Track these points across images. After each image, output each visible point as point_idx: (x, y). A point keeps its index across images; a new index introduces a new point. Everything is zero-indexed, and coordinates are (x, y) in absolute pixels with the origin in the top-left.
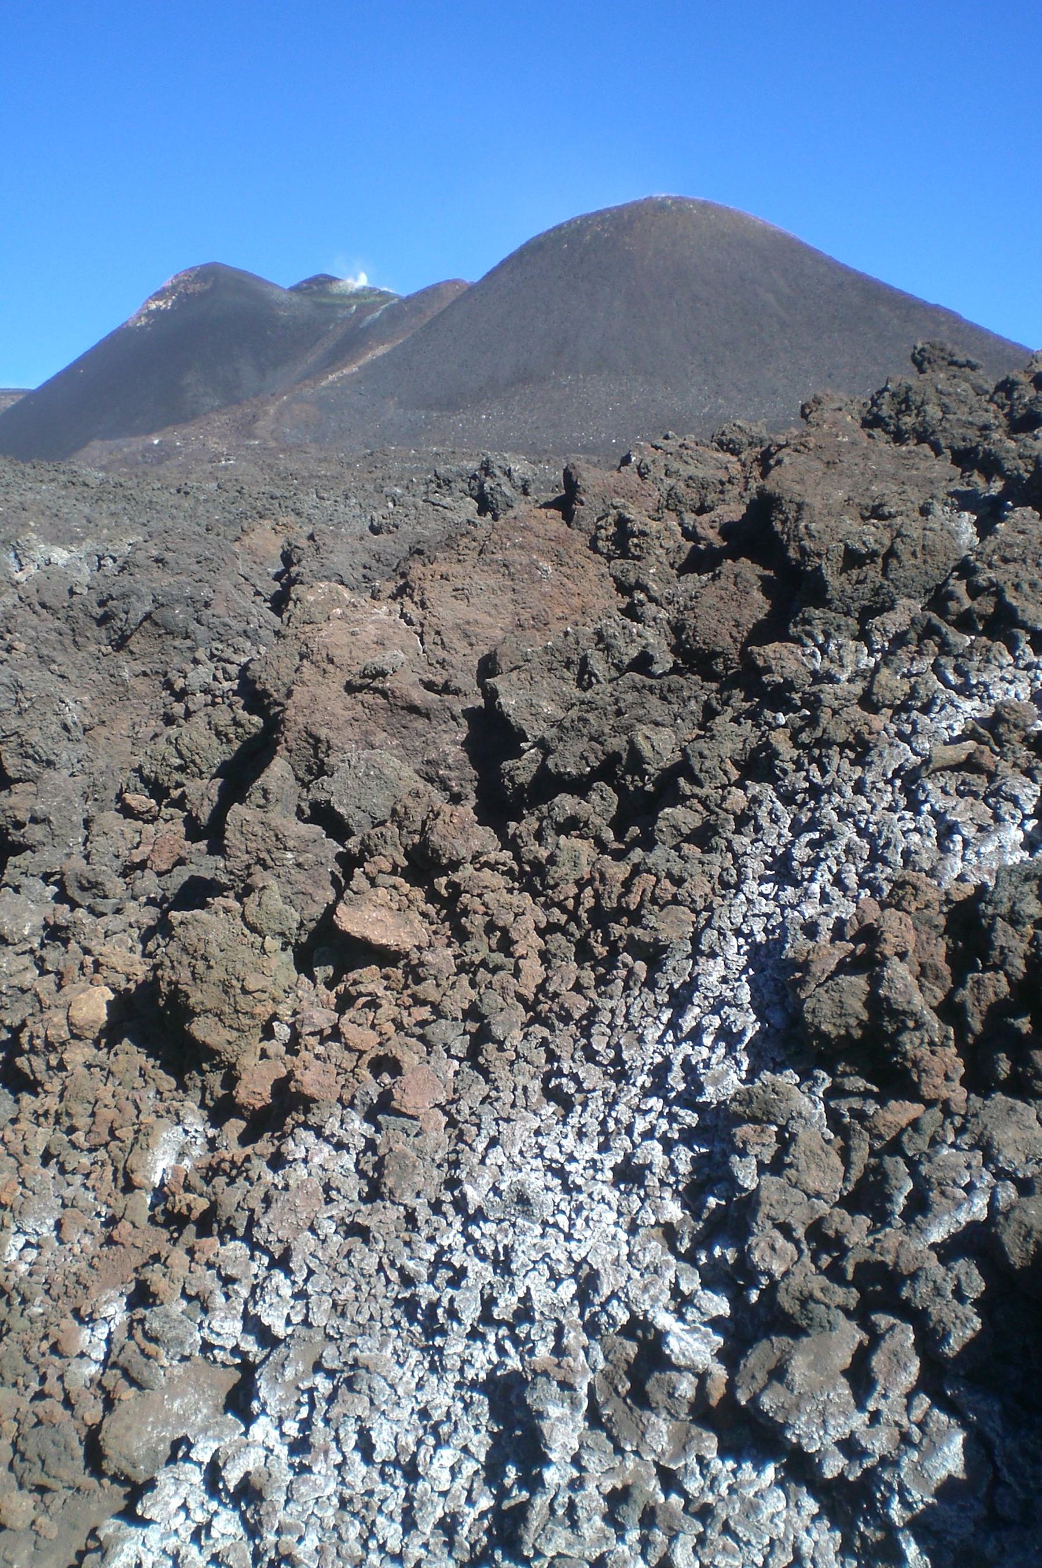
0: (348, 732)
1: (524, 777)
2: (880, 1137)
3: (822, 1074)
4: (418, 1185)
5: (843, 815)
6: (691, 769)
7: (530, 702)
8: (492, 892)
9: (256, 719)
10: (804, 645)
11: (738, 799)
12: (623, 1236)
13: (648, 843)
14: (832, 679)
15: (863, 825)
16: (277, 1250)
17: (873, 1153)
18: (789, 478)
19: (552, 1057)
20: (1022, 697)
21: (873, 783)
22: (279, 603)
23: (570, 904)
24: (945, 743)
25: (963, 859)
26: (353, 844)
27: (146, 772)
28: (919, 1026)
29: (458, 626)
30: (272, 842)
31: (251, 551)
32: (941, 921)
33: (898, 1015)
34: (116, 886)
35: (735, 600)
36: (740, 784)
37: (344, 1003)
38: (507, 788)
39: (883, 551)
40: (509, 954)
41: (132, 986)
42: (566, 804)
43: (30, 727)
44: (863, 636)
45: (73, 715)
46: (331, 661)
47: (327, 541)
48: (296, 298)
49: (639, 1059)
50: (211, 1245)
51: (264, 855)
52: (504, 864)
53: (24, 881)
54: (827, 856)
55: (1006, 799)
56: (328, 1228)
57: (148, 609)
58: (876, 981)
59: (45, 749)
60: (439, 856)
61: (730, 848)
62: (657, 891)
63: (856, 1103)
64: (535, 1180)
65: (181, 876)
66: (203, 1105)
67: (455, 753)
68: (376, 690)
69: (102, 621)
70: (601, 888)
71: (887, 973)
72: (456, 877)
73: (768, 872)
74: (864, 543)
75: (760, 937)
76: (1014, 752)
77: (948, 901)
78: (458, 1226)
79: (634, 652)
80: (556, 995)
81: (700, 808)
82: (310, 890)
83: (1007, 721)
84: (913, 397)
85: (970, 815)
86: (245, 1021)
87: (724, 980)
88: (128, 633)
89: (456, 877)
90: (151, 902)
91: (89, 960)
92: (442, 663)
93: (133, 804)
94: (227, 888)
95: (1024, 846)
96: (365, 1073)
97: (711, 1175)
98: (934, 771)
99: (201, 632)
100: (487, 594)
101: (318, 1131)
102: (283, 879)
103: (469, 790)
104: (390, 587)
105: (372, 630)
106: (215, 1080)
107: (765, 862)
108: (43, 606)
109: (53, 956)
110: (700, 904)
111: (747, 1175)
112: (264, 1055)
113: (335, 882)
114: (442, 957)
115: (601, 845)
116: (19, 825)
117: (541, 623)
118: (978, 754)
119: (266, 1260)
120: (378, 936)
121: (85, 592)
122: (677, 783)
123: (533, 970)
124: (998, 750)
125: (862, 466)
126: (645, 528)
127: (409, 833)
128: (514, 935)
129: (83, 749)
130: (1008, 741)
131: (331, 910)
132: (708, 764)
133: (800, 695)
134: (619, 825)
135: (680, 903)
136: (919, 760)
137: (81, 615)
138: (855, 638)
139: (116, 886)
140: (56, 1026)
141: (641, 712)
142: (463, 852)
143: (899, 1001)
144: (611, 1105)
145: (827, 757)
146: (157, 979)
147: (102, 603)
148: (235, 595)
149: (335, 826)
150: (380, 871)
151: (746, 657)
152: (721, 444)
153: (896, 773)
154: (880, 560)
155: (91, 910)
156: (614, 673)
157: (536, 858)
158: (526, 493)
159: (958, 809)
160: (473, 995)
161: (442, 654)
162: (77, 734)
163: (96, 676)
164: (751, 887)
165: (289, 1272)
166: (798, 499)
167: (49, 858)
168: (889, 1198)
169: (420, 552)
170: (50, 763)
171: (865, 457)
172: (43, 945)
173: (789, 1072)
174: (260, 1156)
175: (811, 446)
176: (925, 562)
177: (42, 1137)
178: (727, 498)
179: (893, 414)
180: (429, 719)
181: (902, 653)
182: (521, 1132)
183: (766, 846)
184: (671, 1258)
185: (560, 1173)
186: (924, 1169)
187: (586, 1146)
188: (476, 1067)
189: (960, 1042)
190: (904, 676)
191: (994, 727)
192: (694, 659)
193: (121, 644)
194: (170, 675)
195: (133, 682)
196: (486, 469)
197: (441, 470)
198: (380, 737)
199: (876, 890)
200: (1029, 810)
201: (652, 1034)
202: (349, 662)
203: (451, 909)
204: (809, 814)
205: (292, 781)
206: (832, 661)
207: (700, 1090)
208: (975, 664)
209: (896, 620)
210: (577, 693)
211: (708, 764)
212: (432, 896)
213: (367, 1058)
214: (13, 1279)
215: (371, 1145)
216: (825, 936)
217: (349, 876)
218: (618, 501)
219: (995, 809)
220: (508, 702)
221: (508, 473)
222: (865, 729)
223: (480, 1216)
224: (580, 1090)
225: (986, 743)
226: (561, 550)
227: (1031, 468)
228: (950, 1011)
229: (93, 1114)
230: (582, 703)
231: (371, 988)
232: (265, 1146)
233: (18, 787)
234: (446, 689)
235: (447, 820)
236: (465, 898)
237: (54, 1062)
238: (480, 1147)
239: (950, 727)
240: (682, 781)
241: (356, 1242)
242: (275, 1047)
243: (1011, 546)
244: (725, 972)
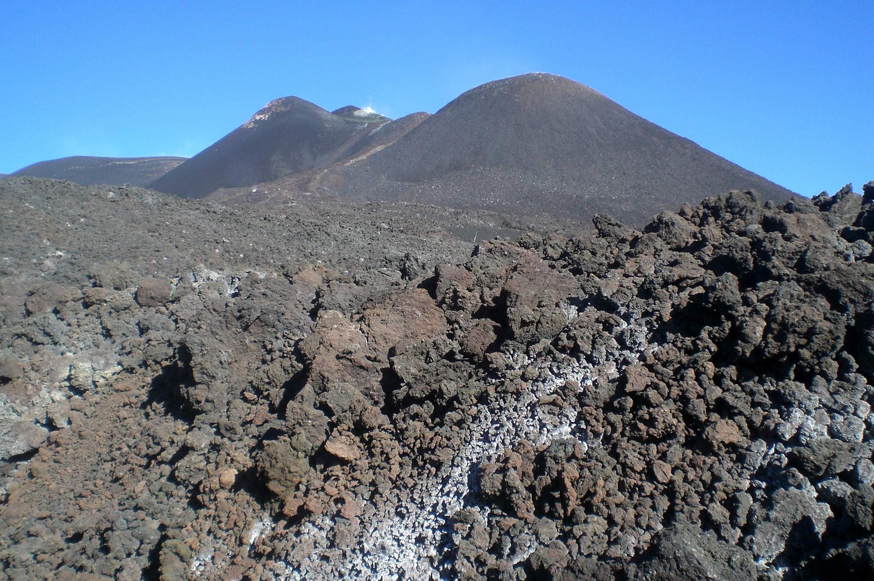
0: (336, 375)
1: (401, 397)
2: (503, 529)
3: (487, 508)
4: (348, 543)
5: (508, 419)
8: (385, 440)
9: (300, 365)
11: (474, 409)
12: (415, 561)
13: (441, 424)
16: (296, 564)
17: (500, 534)
18: (516, 284)
19: (399, 500)
22: (314, 314)
23: (412, 445)
26: (334, 418)
28: (518, 492)
31: (302, 279)
32: (534, 458)
33: (511, 488)
34: (240, 430)
35: (481, 334)
36: (476, 405)
37: (327, 478)
40: (388, 463)
41: (245, 469)
42: (415, 408)
43: (206, 361)
44: (527, 353)
45: (224, 357)
49: (429, 502)
50: (272, 563)
51: (300, 421)
53: (203, 426)
56: (315, 557)
58: (504, 477)
59: (212, 371)
61: (469, 428)
63: (498, 519)
64: (389, 542)
65: (267, 427)
66: (271, 515)
67: (377, 385)
68: (348, 359)
69: (239, 318)
71: (508, 473)
72: (371, 433)
75: (475, 461)
77: (537, 451)
78: (360, 557)
80: (403, 478)
86: (289, 483)
87: (461, 475)
89: (371, 433)
90: (254, 437)
91: (229, 458)
92: (375, 349)
96: (332, 503)
97: (447, 540)
101: (313, 523)
103: (382, 400)
104: (357, 317)
106: (276, 506)
108: (214, 310)
109: (213, 456)
111: (457, 539)
112: (295, 496)
113: (327, 433)
114: (364, 463)
115: (426, 424)
116: (199, 402)
117: (415, 336)
119: (291, 569)
123: (396, 468)
128: (390, 456)
129: (227, 372)
131: (324, 443)
134: (433, 417)
139: (240, 430)
140: (215, 483)
142: (375, 424)
143: (511, 483)
144: (417, 518)
146: (256, 466)
147: (239, 311)
148: (295, 310)
149: (329, 412)
152: (520, 243)
153: (529, 405)
155: (230, 439)
156: (439, 358)
158: (424, 268)
160: (374, 477)
161: (375, 345)
162: (226, 365)
163: (234, 342)
164: (474, 443)
165: (299, 571)
167: (213, 417)
168: (502, 549)
169: (372, 300)
170: (213, 377)
171: (545, 277)
172: (209, 452)
173: (477, 507)
174: (291, 532)
177: (208, 525)
182: (386, 525)
184: (431, 568)
185: (398, 540)
186: (515, 540)
187: (407, 531)
188: (372, 503)
189: (534, 499)
192: (469, 356)
193: (246, 328)
195: (250, 345)
196: (407, 257)
198: (348, 377)
199: (514, 446)
200: (573, 420)
201: (434, 493)
203: (369, 445)
205: (313, 393)
207: (446, 511)
209: (538, 347)
210: (425, 364)
212: (362, 440)
213: (333, 498)
214: (194, 577)
215: (332, 529)
216: (493, 460)
217: (332, 431)
218: (454, 283)
220: (398, 367)
221: (416, 260)
223: (368, 553)
224: (408, 512)
228: (531, 489)
229: (228, 517)
231: (337, 473)
232: (294, 529)
233: (199, 386)
234: (375, 360)
236: (374, 441)
237: (212, 498)
238: (371, 531)
241: (325, 562)
242: (300, 494)
244: (460, 473)
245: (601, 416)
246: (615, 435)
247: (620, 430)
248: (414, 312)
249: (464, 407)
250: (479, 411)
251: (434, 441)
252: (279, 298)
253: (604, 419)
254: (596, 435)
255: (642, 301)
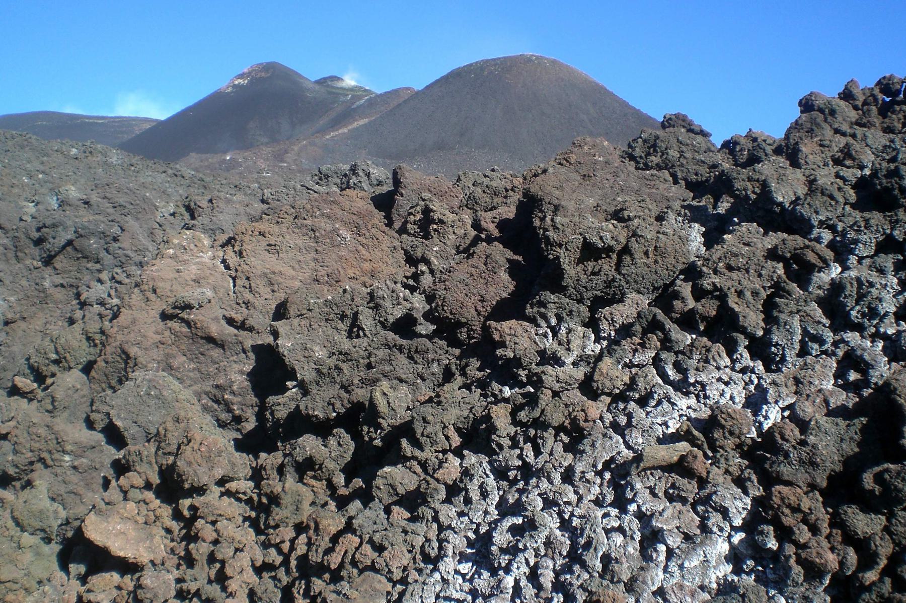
1: (282, 413)
5: (549, 503)
6: (413, 431)
7: (305, 346)
8: (227, 519)
10: (538, 326)
13: (366, 496)
14: (556, 361)
15: (567, 517)
20: (737, 400)
21: (583, 472)
23: (286, 547)
24: (660, 441)
25: (665, 570)
27: (32, 361)
29: (265, 274)
30: (53, 444)
38: (268, 420)
39: (618, 248)
42: (309, 444)
44: (592, 324)
46: (155, 291)
47: (221, 205)
48: (317, 87)
51: (45, 455)
52: (244, 493)
54: (526, 548)
55: (715, 510)
57: (69, 237)
60: (183, 481)
61: (436, 519)
62: (357, 556)
68: (183, 320)
69: (39, 242)
70: (314, 537)
72: (198, 501)
73: (469, 551)
74: (601, 238)
76: (727, 460)
79: (398, 313)
81: (419, 469)
82: (81, 491)
83: (723, 427)
84: (659, 143)
85: (676, 522)
88: (53, 253)
92: (247, 304)
93: (20, 385)
94: (14, 479)
95: (728, 559)
98: (644, 470)
99: (107, 259)
100: (295, 252)
102: (60, 478)
105: (193, 270)
107: (467, 538)
110: (397, 575)
117: (334, 280)
118: (690, 458)
120: (119, 548)
121: (29, 219)
122: (399, 444)
124: (710, 454)
125: (612, 181)
126: (443, 218)
127: (165, 454)
128: (229, 571)
130: (722, 447)
132: (430, 429)
133: (526, 372)
135: (377, 571)
136: (631, 454)
137: (23, 236)
138: (586, 325)
141: (388, 368)
142: (205, 480)
145: (542, 438)
149: (115, 436)
150: (132, 487)
151: (486, 329)
153: (607, 465)
154: (614, 256)
157: (272, 492)
159: (665, 515)
161: (248, 296)
163: (24, 282)
164: (448, 565)
166: (556, 202)
171: (616, 175)
175: (572, 161)
176: (656, 262)
178: (508, 201)
179: (643, 155)
180: (224, 349)
181: (626, 344)
183: (471, 521)
190: (626, 365)
191: (709, 428)
193: (48, 261)
194: (80, 289)
195: (51, 291)
197: (323, 168)
198: (179, 360)
200: (738, 522)
202: (169, 294)
204: (517, 495)
206: (560, 344)
208: (693, 362)
209: (624, 312)
211: (430, 429)
212: (177, 515)
218: (426, 195)
219: (704, 519)
221: (368, 175)
222: (581, 416)
225: (700, 447)
226: (361, 222)
227: (757, 190)
230: (341, 353)
234: (242, 326)
235: (196, 447)
236: (200, 523)
239: (665, 423)
240: (404, 442)
243: (736, 255)
245: (822, 516)
246: (871, 576)
247: (883, 563)
248: (335, 231)
249: (428, 454)
250: (466, 473)
251: (340, 549)
252: (111, 210)
253: (832, 525)
254: (813, 572)
255: (876, 218)
